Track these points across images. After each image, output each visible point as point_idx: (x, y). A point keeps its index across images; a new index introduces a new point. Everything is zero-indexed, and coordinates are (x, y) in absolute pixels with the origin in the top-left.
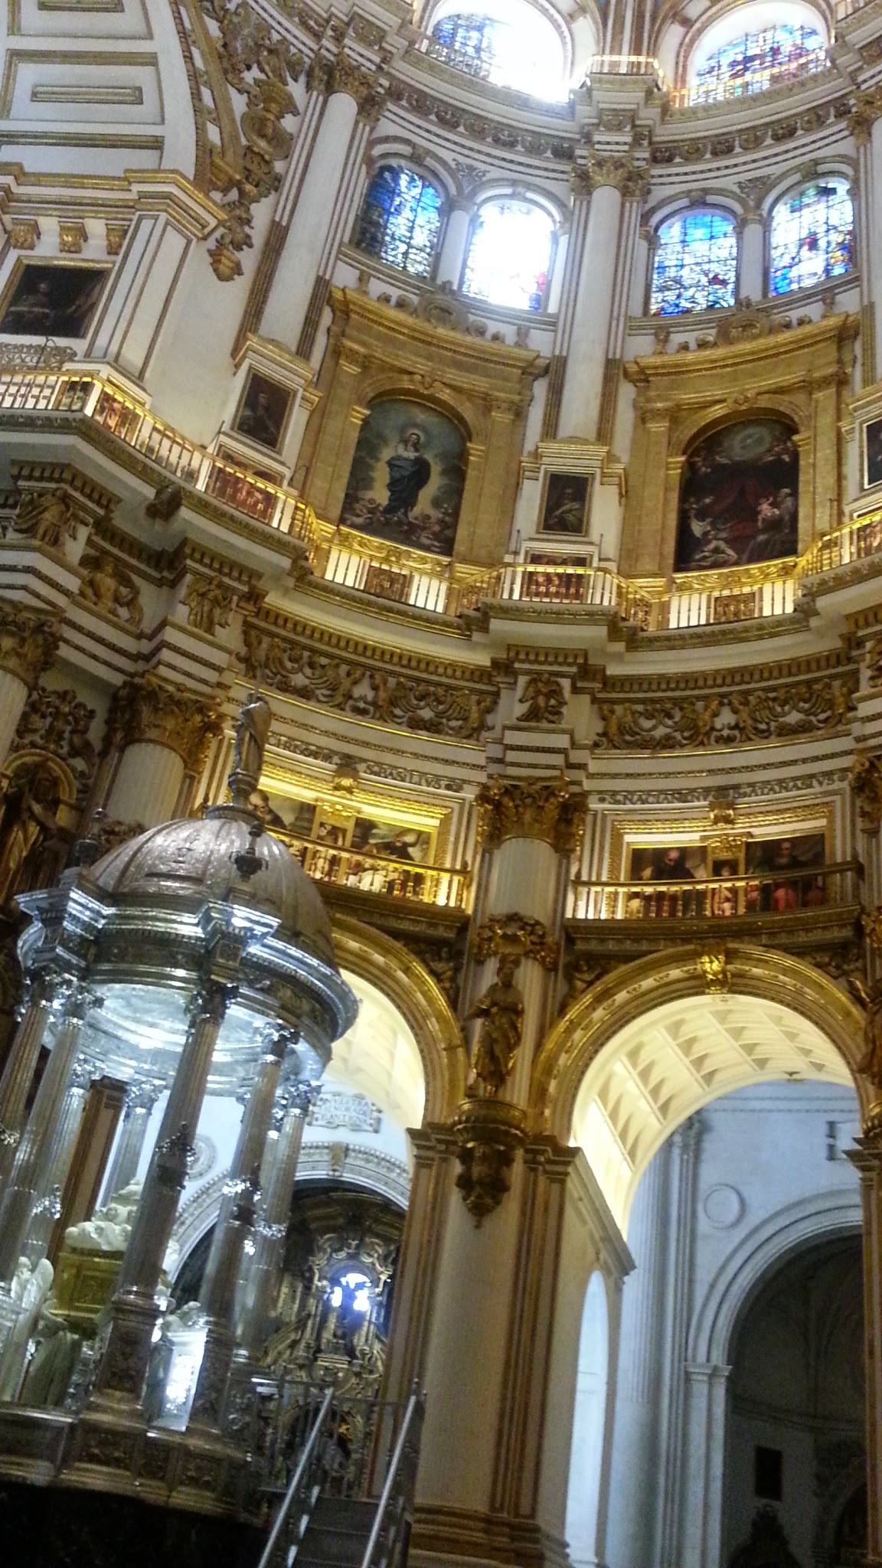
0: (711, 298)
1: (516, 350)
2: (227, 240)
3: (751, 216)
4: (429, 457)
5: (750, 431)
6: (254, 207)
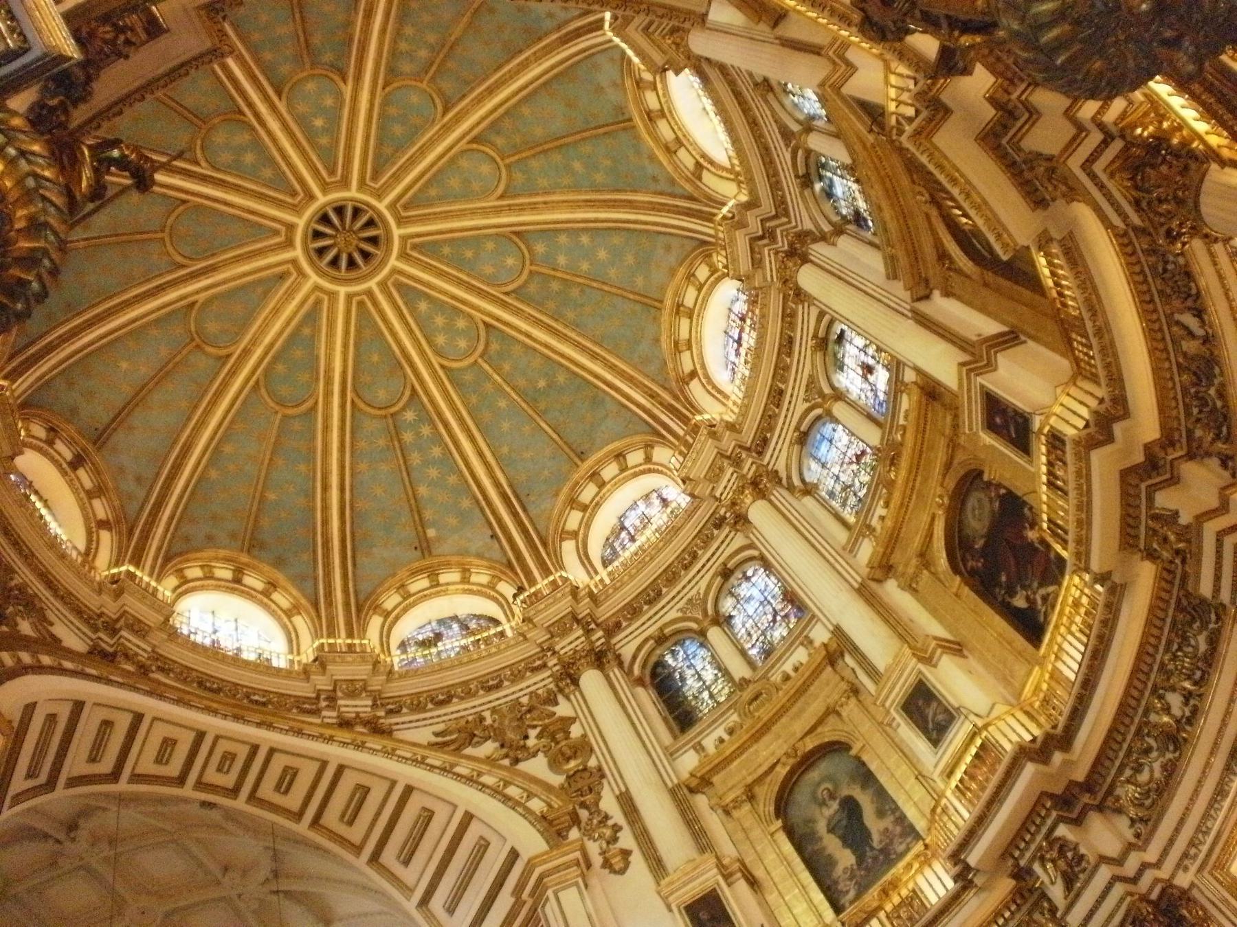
2: (604, 845)
4: (845, 792)
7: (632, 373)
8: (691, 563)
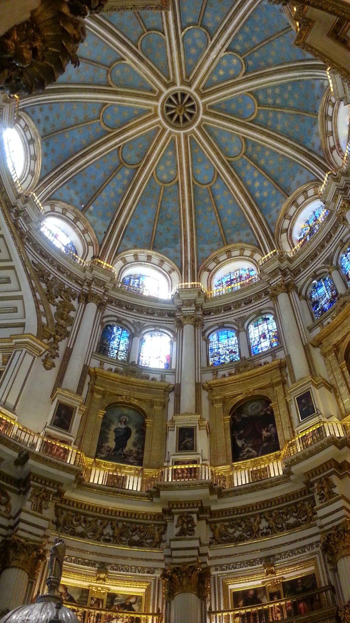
0: (231, 358)
1: (162, 383)
3: (241, 329)
4: (130, 426)
5: (253, 404)
6: (60, 343)
7: (195, 248)
8: (150, 314)
